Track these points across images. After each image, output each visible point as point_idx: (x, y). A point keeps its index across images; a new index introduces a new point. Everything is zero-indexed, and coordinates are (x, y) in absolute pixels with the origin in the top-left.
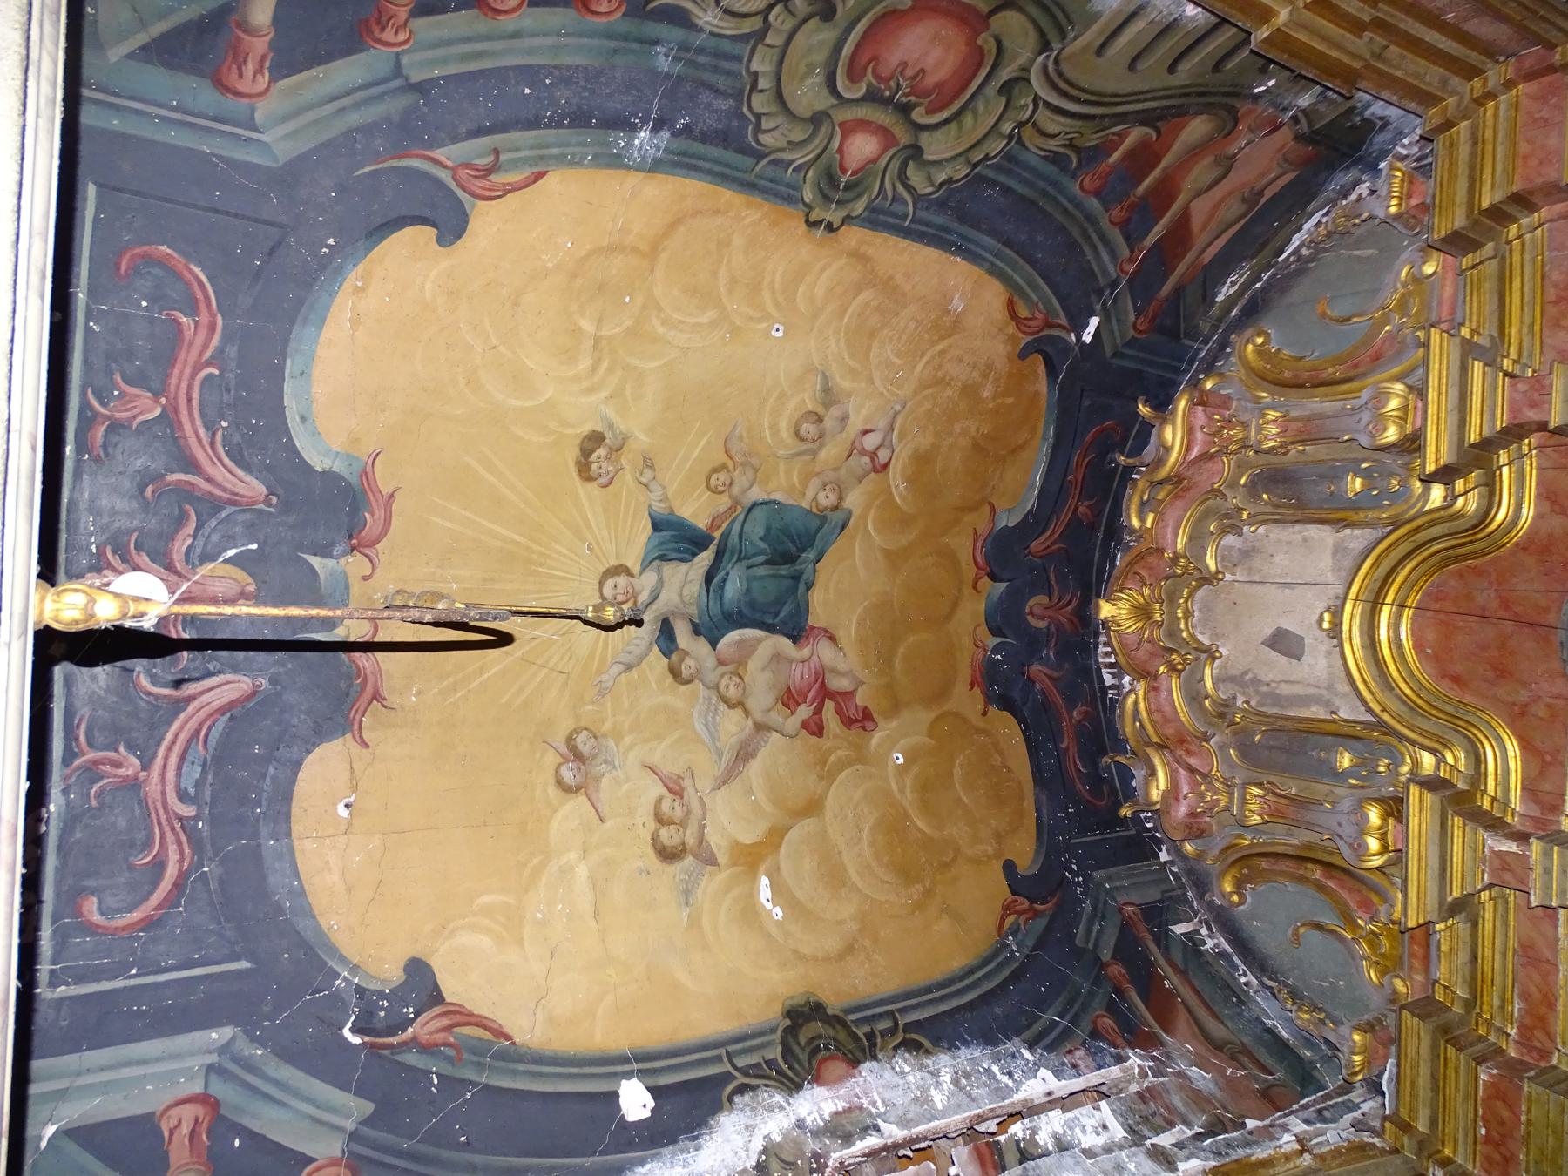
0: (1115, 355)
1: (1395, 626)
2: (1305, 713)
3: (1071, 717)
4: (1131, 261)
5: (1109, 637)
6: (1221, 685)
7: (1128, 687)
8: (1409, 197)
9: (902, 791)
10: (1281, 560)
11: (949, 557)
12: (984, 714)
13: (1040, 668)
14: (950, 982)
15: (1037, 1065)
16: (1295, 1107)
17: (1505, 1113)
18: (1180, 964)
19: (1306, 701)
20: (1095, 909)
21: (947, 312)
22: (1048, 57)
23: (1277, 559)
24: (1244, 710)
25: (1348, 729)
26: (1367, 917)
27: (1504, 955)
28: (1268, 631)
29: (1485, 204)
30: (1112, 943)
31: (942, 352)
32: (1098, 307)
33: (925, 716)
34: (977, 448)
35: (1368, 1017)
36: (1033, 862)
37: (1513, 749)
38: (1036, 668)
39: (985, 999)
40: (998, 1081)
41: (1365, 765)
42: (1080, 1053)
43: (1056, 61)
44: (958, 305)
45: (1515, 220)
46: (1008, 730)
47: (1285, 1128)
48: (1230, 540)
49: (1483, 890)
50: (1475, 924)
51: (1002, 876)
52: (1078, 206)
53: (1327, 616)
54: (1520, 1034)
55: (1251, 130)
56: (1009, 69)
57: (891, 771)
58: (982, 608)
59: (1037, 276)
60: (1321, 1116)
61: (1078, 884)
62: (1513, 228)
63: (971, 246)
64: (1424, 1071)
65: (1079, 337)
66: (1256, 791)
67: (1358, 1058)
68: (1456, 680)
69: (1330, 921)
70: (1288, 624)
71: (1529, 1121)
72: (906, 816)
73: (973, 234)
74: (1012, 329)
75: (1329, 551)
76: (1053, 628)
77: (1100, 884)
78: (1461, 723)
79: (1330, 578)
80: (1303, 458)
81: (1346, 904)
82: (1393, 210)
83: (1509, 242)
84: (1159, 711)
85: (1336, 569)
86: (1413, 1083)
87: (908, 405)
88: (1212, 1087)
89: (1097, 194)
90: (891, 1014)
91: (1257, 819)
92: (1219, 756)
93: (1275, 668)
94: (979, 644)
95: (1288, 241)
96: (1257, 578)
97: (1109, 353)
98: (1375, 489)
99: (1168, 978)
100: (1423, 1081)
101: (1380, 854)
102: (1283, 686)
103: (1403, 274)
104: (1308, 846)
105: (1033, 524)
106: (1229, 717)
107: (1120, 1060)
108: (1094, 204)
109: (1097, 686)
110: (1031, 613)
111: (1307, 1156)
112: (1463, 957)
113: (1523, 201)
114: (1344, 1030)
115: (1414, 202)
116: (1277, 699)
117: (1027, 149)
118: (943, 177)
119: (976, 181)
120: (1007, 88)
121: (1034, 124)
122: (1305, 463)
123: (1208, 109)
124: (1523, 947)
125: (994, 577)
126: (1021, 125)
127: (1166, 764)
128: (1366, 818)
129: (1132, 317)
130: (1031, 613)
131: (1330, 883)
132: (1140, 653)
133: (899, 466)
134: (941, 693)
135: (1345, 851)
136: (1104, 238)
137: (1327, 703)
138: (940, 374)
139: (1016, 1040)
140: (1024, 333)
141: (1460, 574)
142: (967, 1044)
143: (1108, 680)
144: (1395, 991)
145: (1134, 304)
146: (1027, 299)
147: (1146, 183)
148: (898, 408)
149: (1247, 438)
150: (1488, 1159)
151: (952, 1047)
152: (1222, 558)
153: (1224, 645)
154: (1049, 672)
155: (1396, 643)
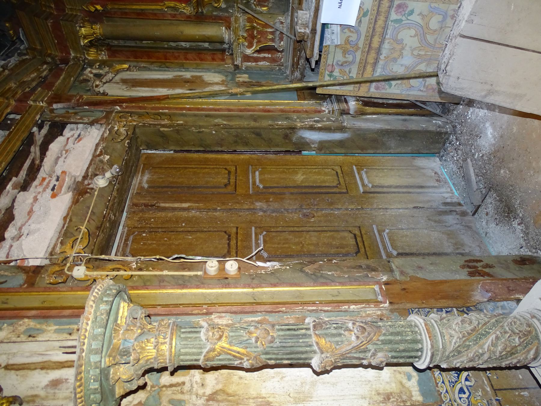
67: (11, 32)
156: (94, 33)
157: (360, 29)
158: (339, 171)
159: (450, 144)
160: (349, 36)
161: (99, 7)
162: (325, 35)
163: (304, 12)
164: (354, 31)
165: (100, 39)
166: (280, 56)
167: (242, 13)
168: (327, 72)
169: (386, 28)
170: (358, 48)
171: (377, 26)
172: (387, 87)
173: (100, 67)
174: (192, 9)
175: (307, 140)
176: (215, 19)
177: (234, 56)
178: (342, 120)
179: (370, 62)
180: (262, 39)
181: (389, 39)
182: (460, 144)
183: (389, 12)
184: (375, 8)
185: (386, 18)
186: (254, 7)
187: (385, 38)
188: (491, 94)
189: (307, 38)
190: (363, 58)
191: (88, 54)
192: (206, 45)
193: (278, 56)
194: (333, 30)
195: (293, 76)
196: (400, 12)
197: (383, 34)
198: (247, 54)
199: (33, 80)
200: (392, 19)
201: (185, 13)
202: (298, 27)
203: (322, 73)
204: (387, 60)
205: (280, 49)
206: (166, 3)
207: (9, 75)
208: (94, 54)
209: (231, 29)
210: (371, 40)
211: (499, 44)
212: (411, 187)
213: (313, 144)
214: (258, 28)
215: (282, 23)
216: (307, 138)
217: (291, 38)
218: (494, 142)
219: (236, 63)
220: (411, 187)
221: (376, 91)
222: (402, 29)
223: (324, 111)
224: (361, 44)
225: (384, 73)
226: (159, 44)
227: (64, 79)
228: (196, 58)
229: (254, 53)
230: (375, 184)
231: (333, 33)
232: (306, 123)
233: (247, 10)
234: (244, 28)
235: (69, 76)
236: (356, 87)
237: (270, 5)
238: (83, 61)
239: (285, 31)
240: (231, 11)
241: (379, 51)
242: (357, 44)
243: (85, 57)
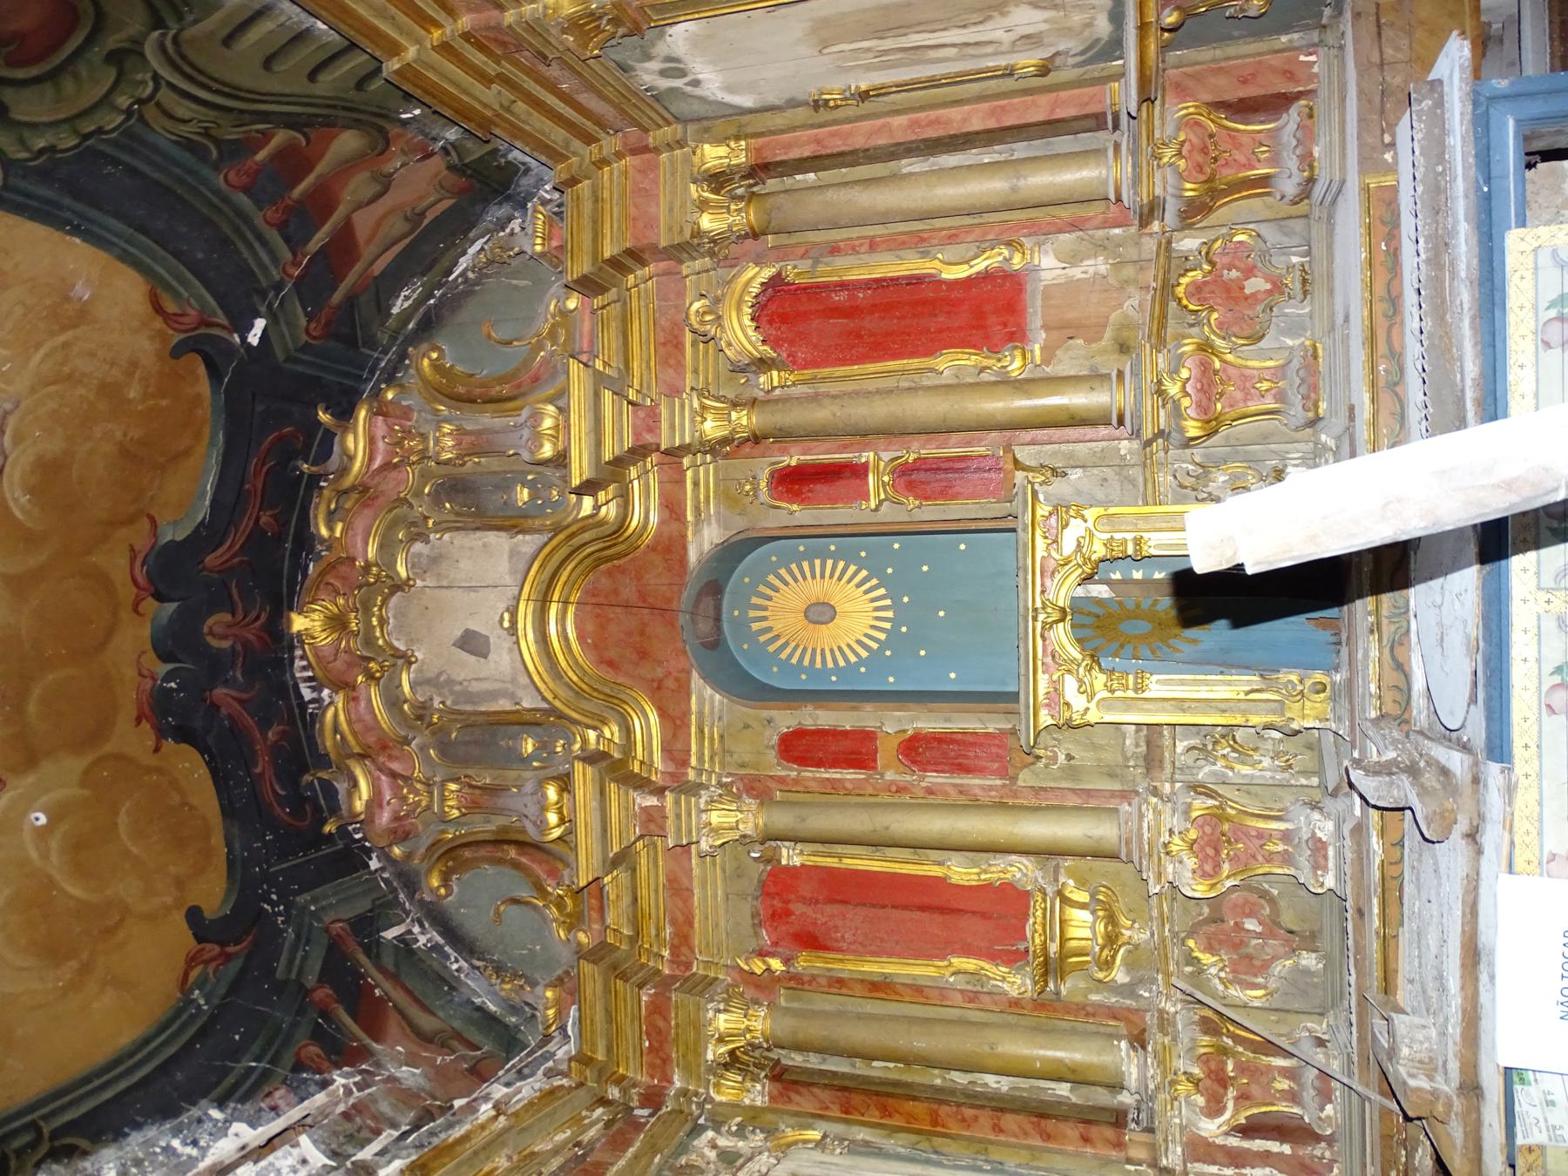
0: (287, 360)
1: (562, 620)
2: (494, 707)
3: (265, 738)
4: (296, 264)
5: (304, 650)
6: (418, 688)
7: (327, 700)
8: (550, 239)
9: (45, 856)
10: (465, 565)
11: (101, 580)
12: (157, 750)
13: (225, 691)
14: (117, 1062)
15: (228, 1122)
16: (501, 1073)
17: (661, 1024)
18: (391, 968)
19: (493, 695)
20: (298, 937)
21: (67, 299)
22: (164, 35)
23: (462, 565)
24: (440, 710)
25: (528, 717)
26: (553, 883)
27: (656, 891)
28: (458, 633)
29: (607, 255)
30: (318, 967)
31: (65, 345)
32: (263, 309)
33: (75, 765)
34: (126, 453)
35: (559, 972)
36: (225, 901)
37: (654, 718)
38: (220, 692)
39: (164, 1068)
40: (179, 1156)
41: (544, 746)
42: (278, 1094)
43: (175, 40)
44: (83, 292)
45: (632, 271)
46: (190, 766)
47: (487, 1098)
48: (418, 547)
49: (638, 839)
50: (634, 870)
51: (185, 926)
52: (226, 200)
53: (506, 616)
54: (672, 954)
55: (404, 152)
56: (118, 37)
57: (27, 836)
58: (146, 632)
59: (182, 268)
60: (521, 1075)
61: (280, 914)
62: (631, 277)
63: (95, 229)
64: (599, 1008)
65: (244, 339)
66: (453, 787)
67: (551, 1012)
68: (611, 664)
69: (525, 893)
70: (474, 626)
71: (677, 1024)
72: (51, 883)
73: (94, 213)
74: (158, 323)
75: (506, 557)
76: (239, 648)
77: (305, 907)
78: (616, 701)
79: (508, 580)
80: (479, 469)
81: (538, 877)
82: (538, 248)
83: (628, 290)
84: (360, 720)
85: (513, 572)
86: (592, 1021)
87: (23, 405)
88: (422, 1081)
89: (246, 190)
90: (34, 1126)
91: (456, 813)
92: (419, 759)
93: (466, 668)
94: (146, 673)
95: (456, 264)
96: (445, 583)
97: (280, 354)
98: (539, 498)
99: (377, 986)
100: (599, 1016)
101: (558, 826)
102: (474, 683)
103: (552, 307)
104: (504, 829)
105: (206, 536)
106: (427, 719)
107: (324, 1084)
108: (243, 199)
109: (294, 703)
110: (211, 633)
111: (502, 1118)
112: (626, 900)
113: (636, 256)
114: (539, 989)
115: (555, 243)
116: (470, 697)
117: (153, 130)
118: (41, 144)
119: (89, 155)
120: (116, 58)
121: (158, 105)
122: (482, 474)
123: (356, 124)
124: (669, 880)
125: (159, 597)
126: (140, 101)
127: (368, 773)
128: (545, 796)
129: (303, 321)
130: (211, 633)
131: (523, 860)
132: (338, 664)
133: (17, 475)
134: (98, 733)
135: (531, 829)
136: (260, 238)
137: (512, 696)
138: (66, 369)
139: (203, 1102)
140: (175, 329)
141: (609, 573)
142: (138, 1126)
143: (307, 694)
144: (579, 944)
145: (304, 308)
146: (177, 296)
147: (302, 187)
148: (8, 406)
149: (426, 449)
150: (652, 1066)
151: (118, 1135)
152: (412, 565)
153: (419, 650)
154: (234, 693)
155: (563, 636)
156: (748, 1030)
161: (776, 964)
163: (1417, 1020)
165: (760, 1047)
166: (1327, 1154)
167: (1182, 1001)
173: (740, 1133)
174: (1028, 982)
176: (1094, 1015)
177: (1160, 1137)
180: (1255, 1090)
186: (1221, 987)
189: (1448, 1113)
191: (717, 1086)
192: (1063, 1090)
193: (1318, 1153)
198: (1203, 1134)
199: (556, 1152)
201: (1005, 994)
202: (1402, 1070)
205: (1325, 1130)
206: (953, 960)
207: (505, 1130)
208: (733, 1088)
209: (1150, 1048)
214: (1242, 1053)
215: (1321, 1043)
217: (1363, 1099)
219: (1164, 1162)
226: (917, 1076)
227: (636, 1157)
228: (1029, 1127)
229: (1227, 1134)
231: (1550, 1103)
233: (1199, 996)
234: (1191, 1049)
235: (652, 1148)
237: (1273, 985)
238: (700, 1105)
239: (1335, 1067)
240: (1147, 995)
243: (708, 1093)
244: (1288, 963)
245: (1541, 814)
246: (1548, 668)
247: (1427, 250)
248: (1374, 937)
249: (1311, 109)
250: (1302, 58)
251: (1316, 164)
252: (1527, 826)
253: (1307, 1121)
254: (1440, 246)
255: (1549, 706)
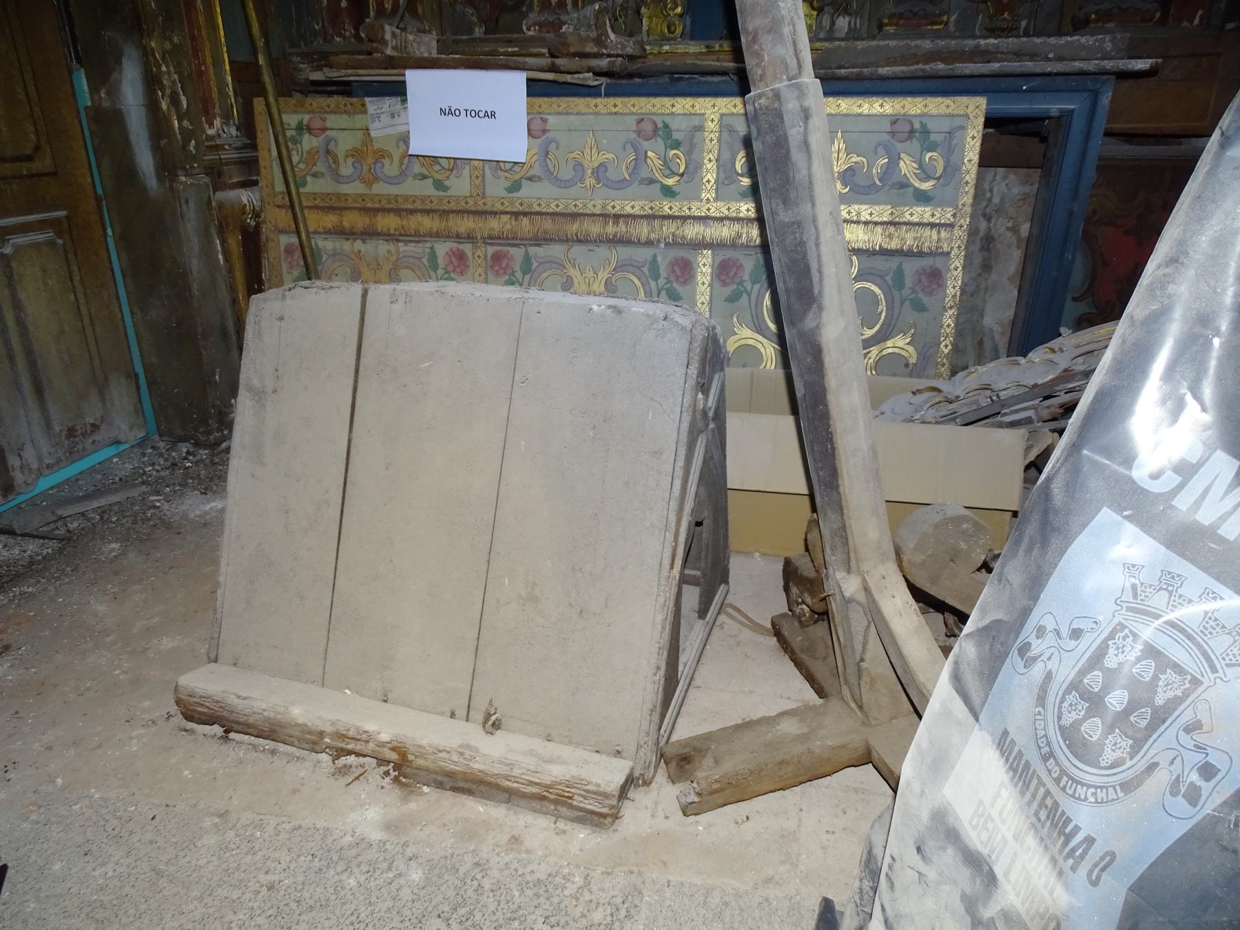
157: (410, 179)
158: (36, 166)
159: (188, 453)
160: (390, 156)
162: (386, 98)
164: (404, 167)
168: (306, 118)
169: (417, 239)
170: (369, 184)
171: (419, 217)
172: (296, 273)
175: (115, 75)
178: (194, 172)
179: (345, 218)
181: (397, 250)
182: (187, 468)
183: (448, 237)
184: (453, 206)
185: (437, 232)
187: (399, 241)
188: (257, 398)
190: (350, 201)
193: (347, 26)
194: (399, 116)
195: (299, 59)
196: (451, 262)
197: (407, 235)
200: (437, 246)
203: (302, 106)
204: (354, 256)
210: (389, 211)
211: (357, 371)
212: (32, 363)
213: (108, 93)
216: (121, 72)
218: (192, 516)
220: (32, 363)
221: (282, 249)
222: (417, 272)
223: (211, 125)
224: (380, 188)
225: (325, 257)
230: (14, 264)
231: (393, 116)
232: (164, 68)
236: (283, 198)
241: (370, 234)
242: (377, 179)
244: (474, 19)
245: (572, 114)
246: (668, 120)
247: (987, 45)
248: (492, 48)
249: (1150, 20)
250: (1200, 12)
251: (1099, 24)
252: (564, 105)
253: (367, 20)
254: (986, 56)
255: (643, 120)
